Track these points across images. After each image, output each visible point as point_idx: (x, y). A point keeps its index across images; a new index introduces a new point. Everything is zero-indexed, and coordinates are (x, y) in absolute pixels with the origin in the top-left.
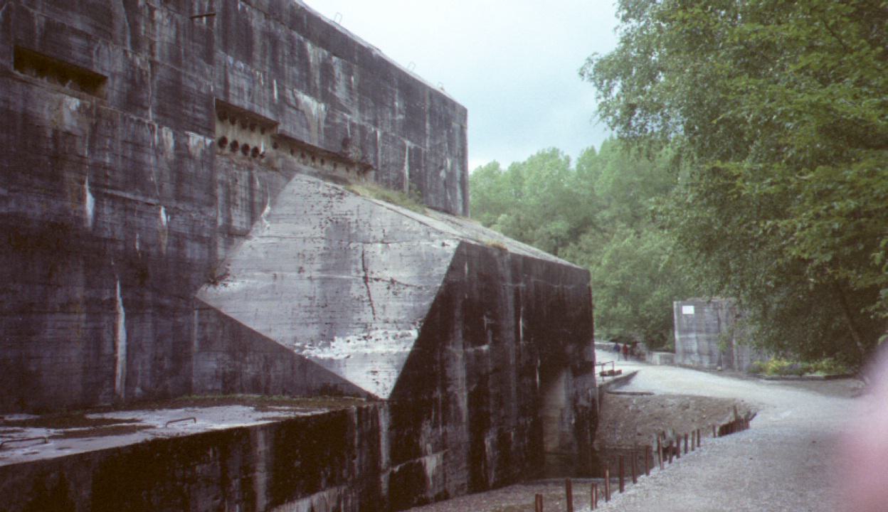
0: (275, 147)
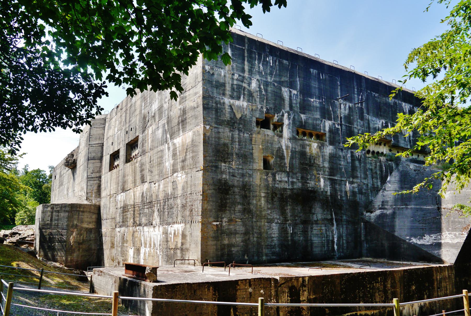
0: (390, 150)
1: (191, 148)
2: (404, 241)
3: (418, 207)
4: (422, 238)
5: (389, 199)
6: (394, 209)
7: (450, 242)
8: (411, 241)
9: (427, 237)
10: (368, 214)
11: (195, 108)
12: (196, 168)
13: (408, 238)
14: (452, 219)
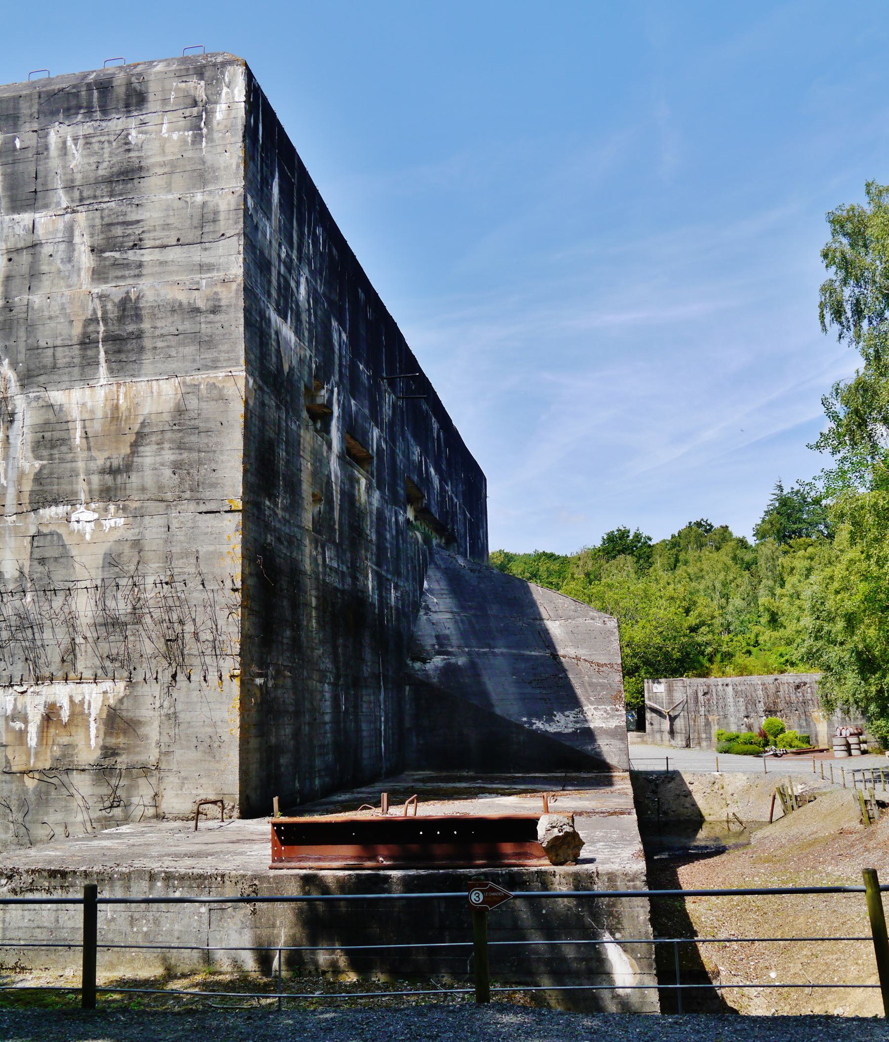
1: (168, 435)
2: (520, 726)
3: (514, 651)
4: (553, 721)
5: (447, 632)
6: (469, 654)
7: (604, 725)
8: (534, 727)
9: (559, 716)
10: (418, 665)
11: (197, 310)
12: (198, 501)
13: (525, 719)
14: (586, 678)
